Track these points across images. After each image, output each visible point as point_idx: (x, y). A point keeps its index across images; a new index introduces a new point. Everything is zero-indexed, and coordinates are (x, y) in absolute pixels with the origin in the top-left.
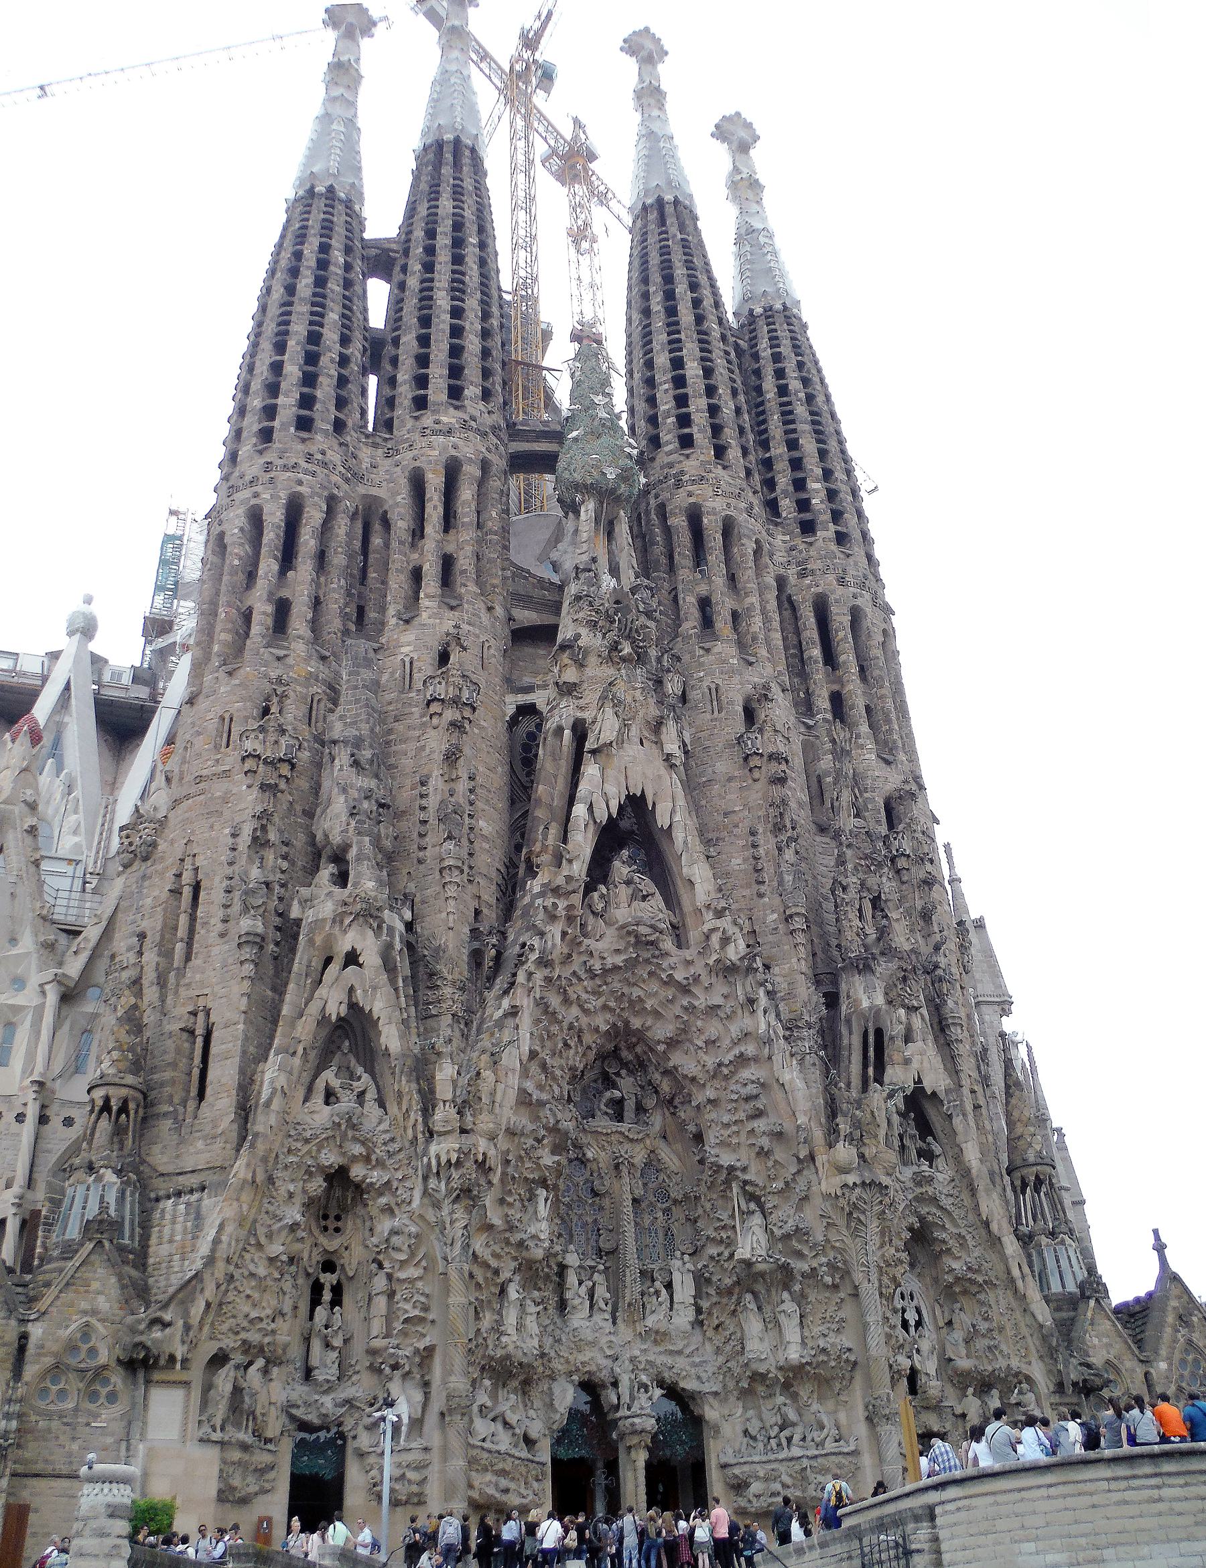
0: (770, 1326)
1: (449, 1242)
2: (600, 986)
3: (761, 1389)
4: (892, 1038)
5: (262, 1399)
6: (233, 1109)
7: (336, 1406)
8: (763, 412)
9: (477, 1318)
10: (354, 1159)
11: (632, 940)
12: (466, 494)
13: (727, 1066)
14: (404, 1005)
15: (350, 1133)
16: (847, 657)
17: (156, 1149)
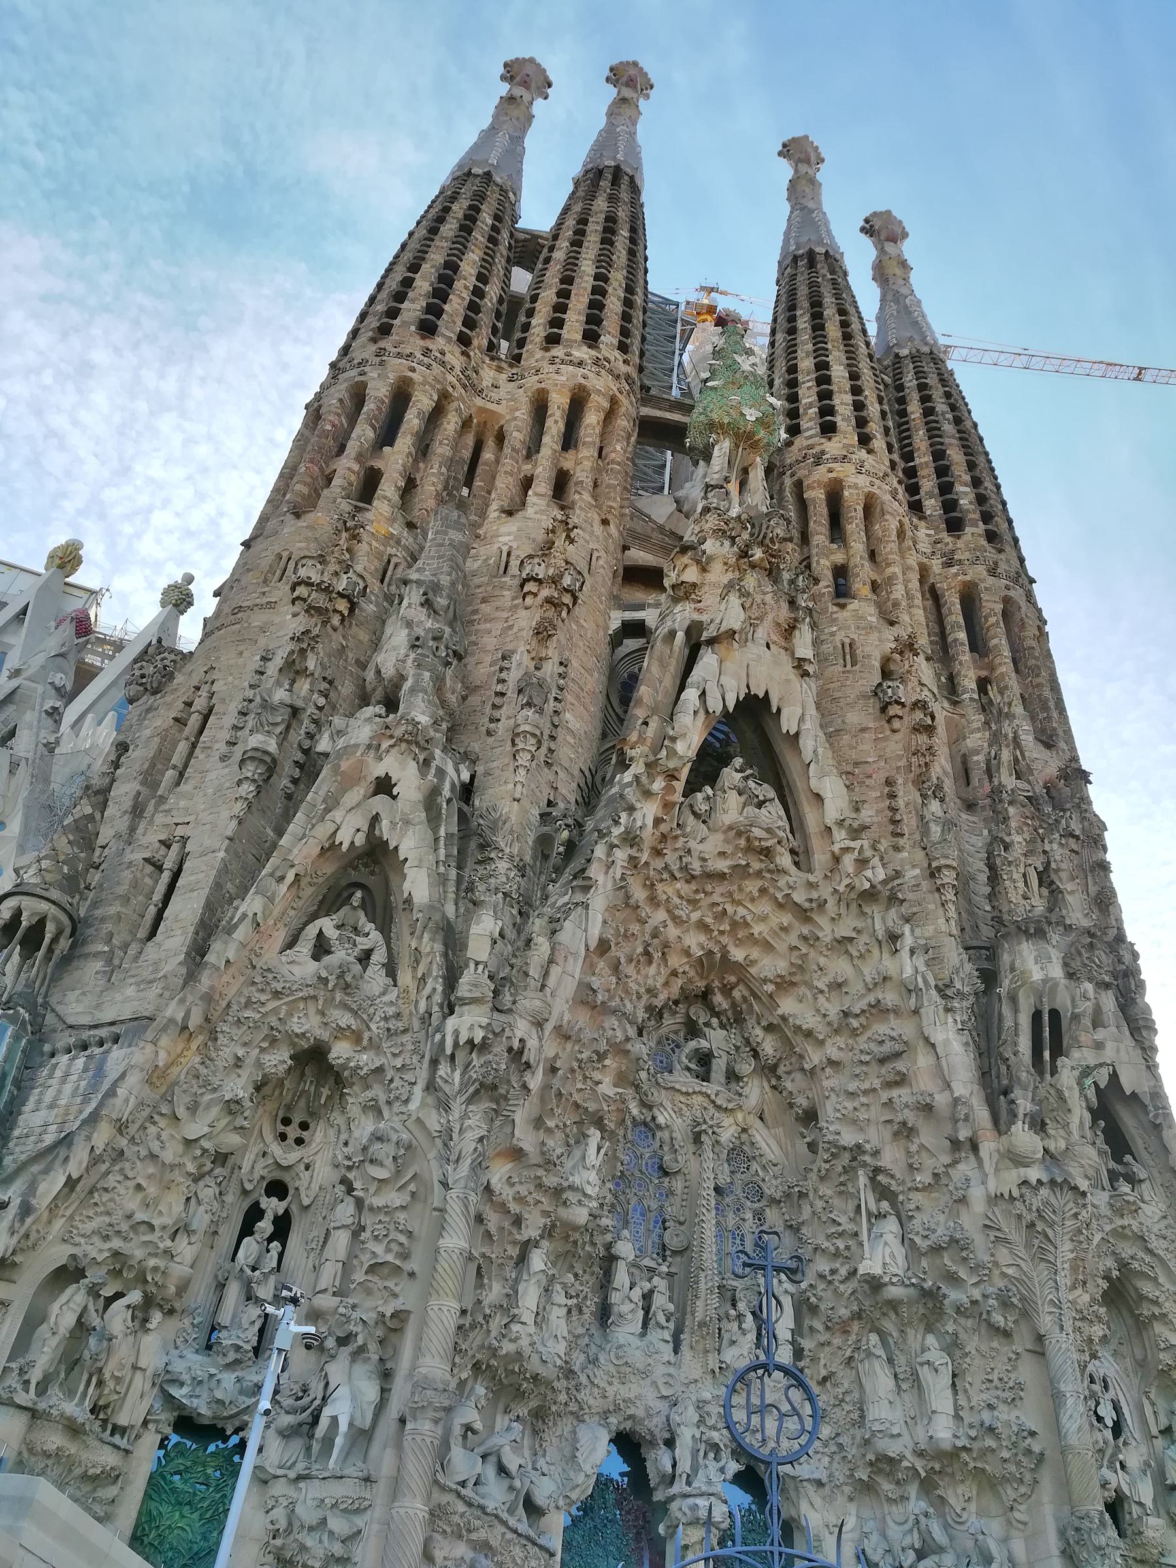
0: (904, 1386)
1: (453, 1158)
2: (697, 891)
3: (886, 1486)
4: (1076, 1017)
5: (123, 1351)
6: (185, 949)
7: (242, 1392)
8: (908, 430)
9: (480, 1285)
10: (341, 1032)
11: (742, 842)
12: (592, 419)
13: (857, 1016)
14: (442, 858)
15: (339, 996)
16: (999, 641)
17: (71, 996)
